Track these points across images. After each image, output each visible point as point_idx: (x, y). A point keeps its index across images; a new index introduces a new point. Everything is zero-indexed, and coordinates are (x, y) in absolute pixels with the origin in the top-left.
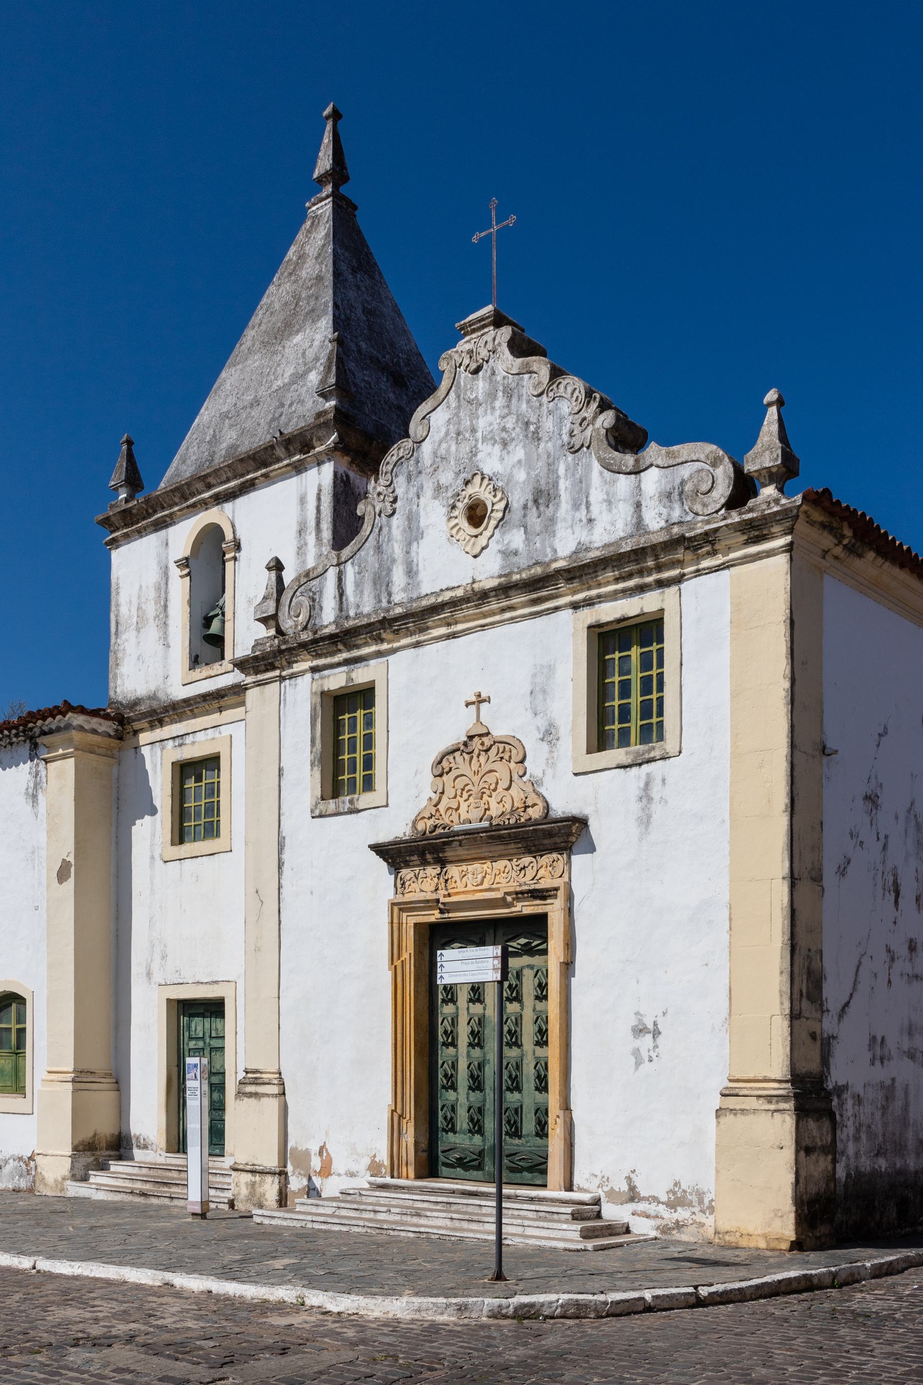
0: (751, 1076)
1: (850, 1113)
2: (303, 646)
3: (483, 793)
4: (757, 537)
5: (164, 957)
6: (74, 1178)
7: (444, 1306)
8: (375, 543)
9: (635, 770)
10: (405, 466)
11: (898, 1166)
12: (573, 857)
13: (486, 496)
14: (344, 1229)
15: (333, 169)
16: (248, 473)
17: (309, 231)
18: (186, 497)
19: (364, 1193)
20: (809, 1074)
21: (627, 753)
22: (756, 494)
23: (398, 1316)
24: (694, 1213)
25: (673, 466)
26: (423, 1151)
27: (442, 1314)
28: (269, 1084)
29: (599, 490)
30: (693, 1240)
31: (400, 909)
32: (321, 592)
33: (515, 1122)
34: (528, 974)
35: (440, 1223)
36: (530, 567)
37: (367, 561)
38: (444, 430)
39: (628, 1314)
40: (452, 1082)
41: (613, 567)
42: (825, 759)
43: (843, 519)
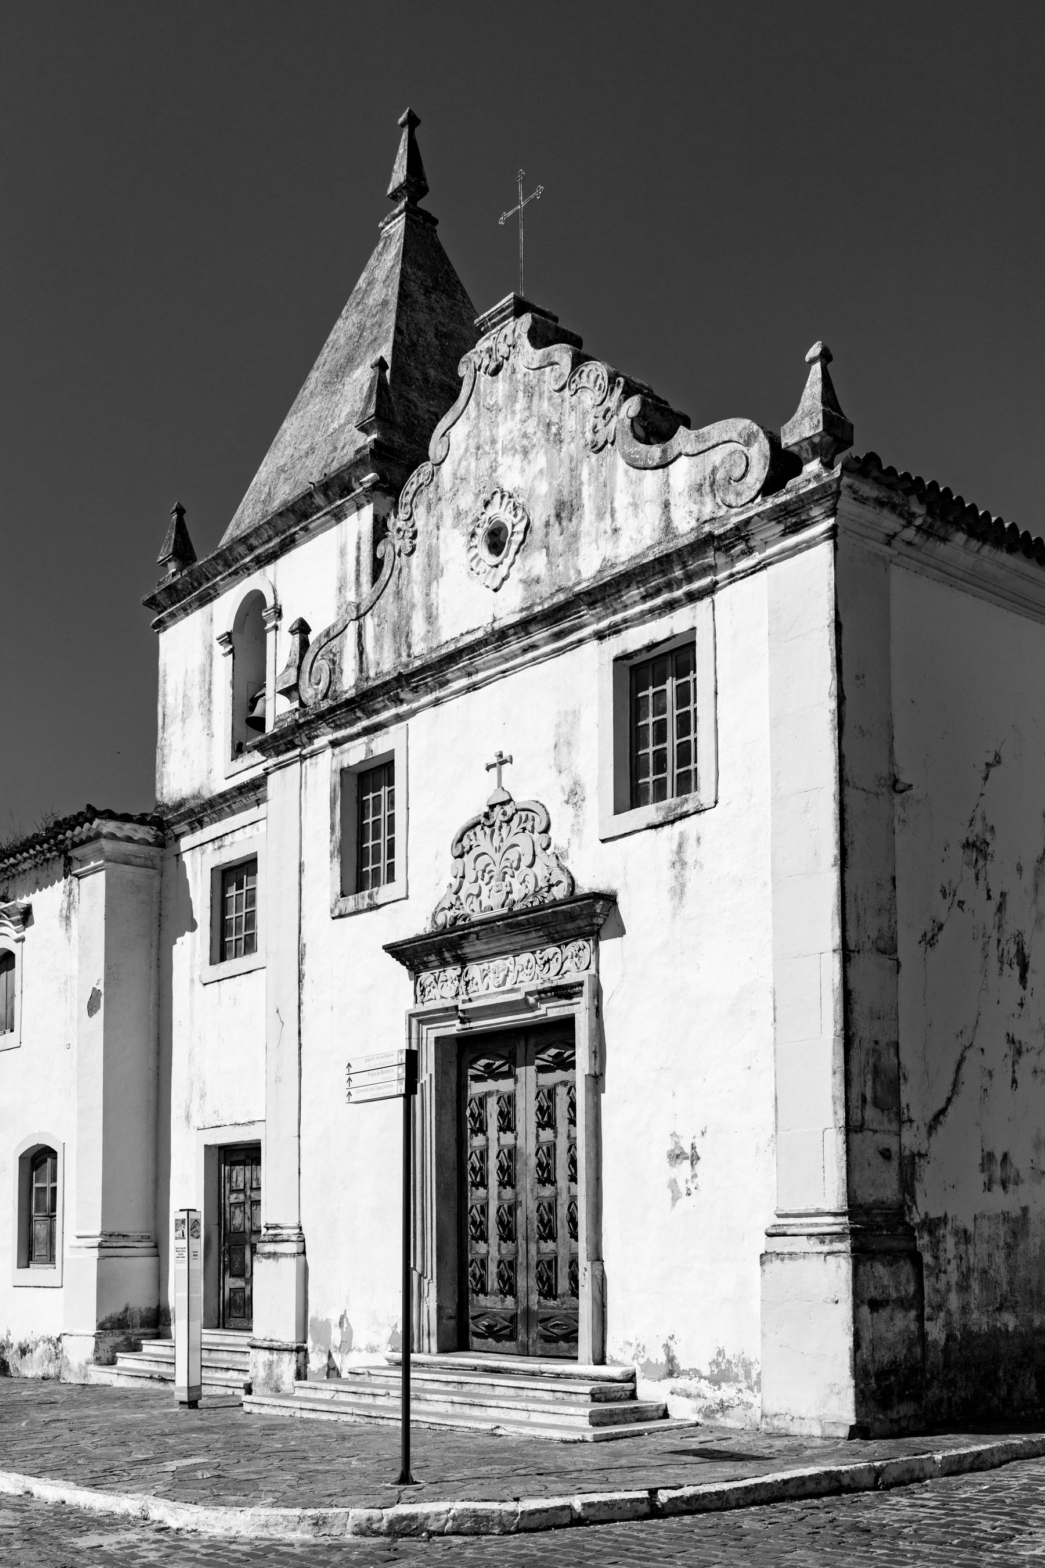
0: (801, 1208)
1: (950, 1255)
2: (321, 716)
3: (505, 873)
4: (795, 524)
5: (202, 1096)
6: (98, 1361)
7: (297, 1519)
8: (394, 588)
9: (667, 828)
10: (424, 493)
11: (1037, 1323)
13: (506, 517)
14: (333, 1417)
15: (407, 180)
16: (290, 528)
17: (380, 254)
18: (234, 562)
19: (372, 1372)
20: (880, 1204)
21: (657, 810)
22: (798, 472)
23: (242, 1533)
24: (740, 1390)
25: (704, 452)
26: (450, 1318)
27: (294, 1530)
28: (287, 1241)
29: (624, 492)
30: (739, 1425)
32: (341, 652)
33: (549, 1278)
34: (562, 1091)
35: (442, 1408)
36: (552, 595)
37: (386, 610)
38: (463, 446)
39: (548, 1528)
40: (482, 1230)
41: (638, 582)
42: (898, 799)
43: (908, 492)
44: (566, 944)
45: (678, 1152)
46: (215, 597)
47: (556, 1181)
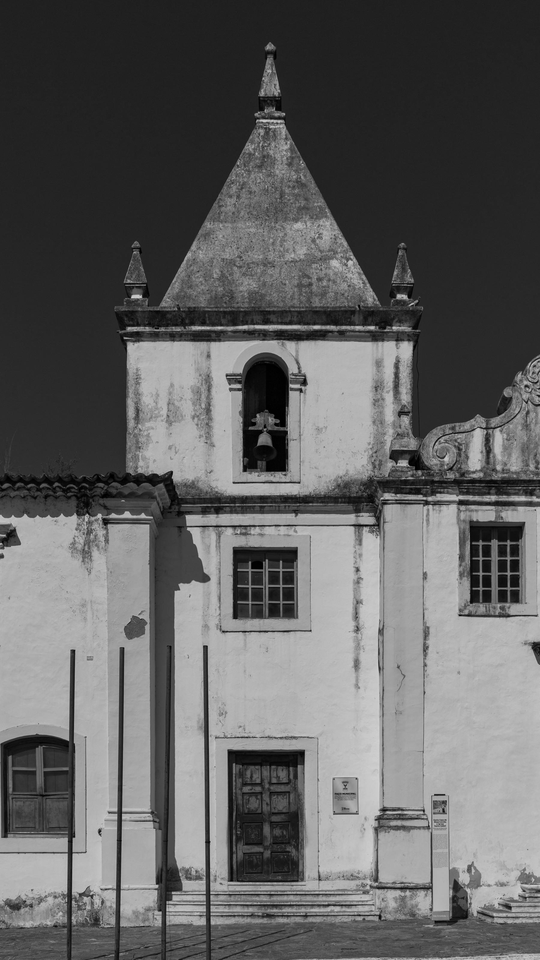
32: (467, 445)
46: (215, 340)
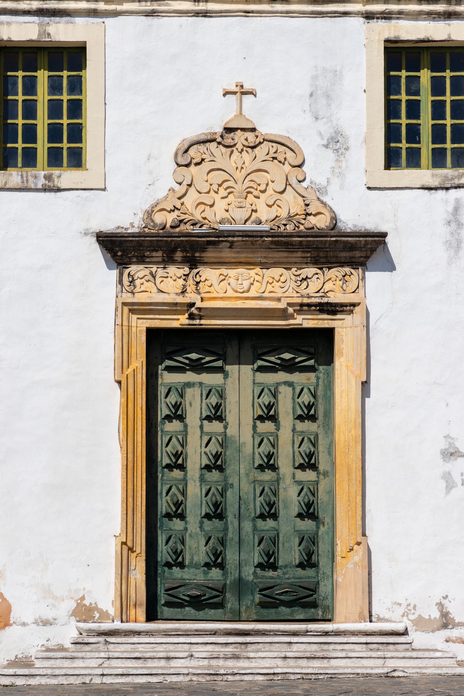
12: (367, 273)
31: (130, 310)
44: (330, 268)
45: (452, 451)
47: (278, 468)
